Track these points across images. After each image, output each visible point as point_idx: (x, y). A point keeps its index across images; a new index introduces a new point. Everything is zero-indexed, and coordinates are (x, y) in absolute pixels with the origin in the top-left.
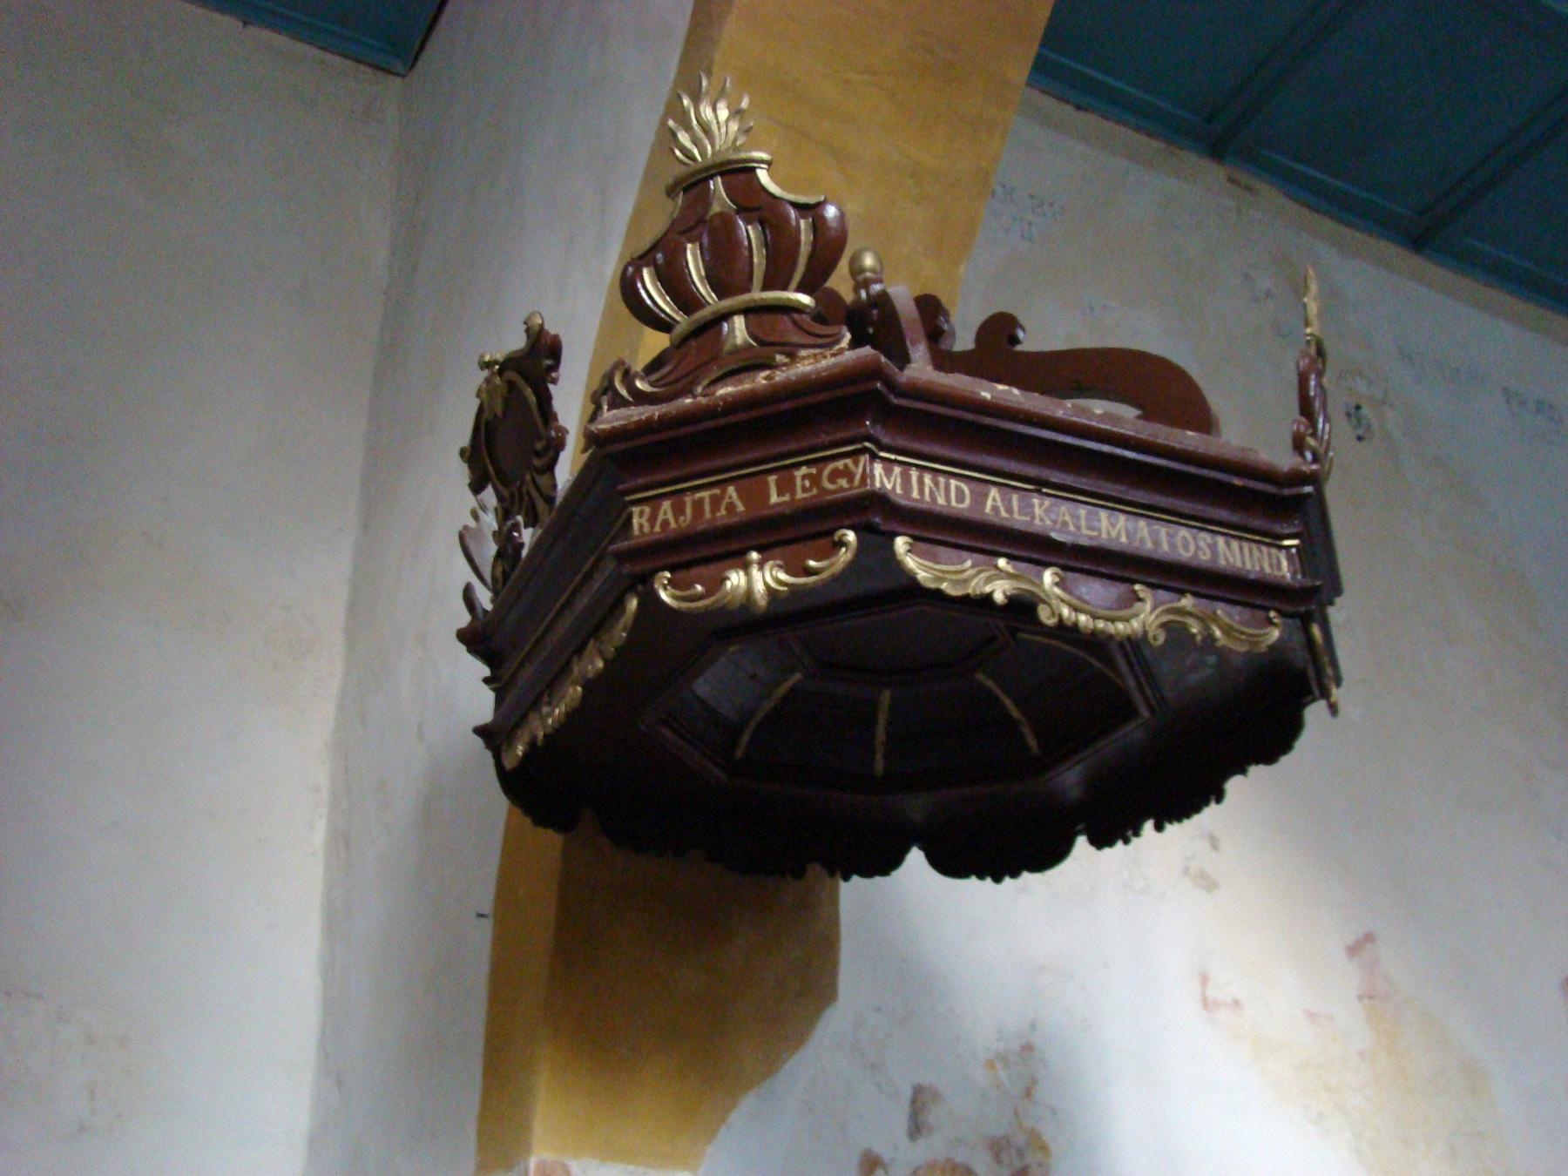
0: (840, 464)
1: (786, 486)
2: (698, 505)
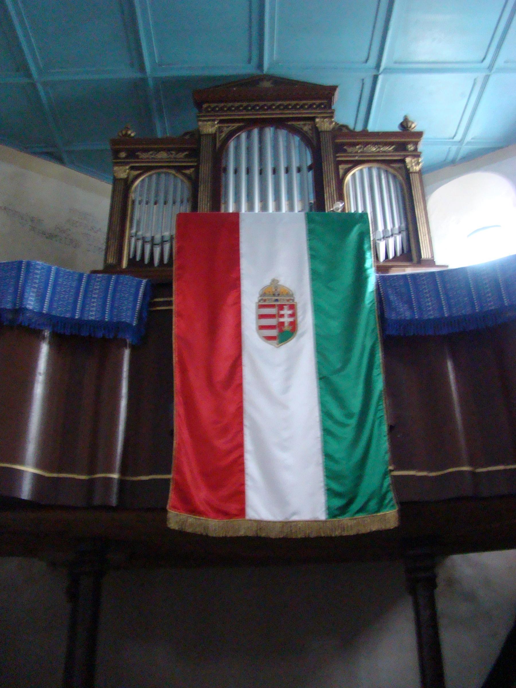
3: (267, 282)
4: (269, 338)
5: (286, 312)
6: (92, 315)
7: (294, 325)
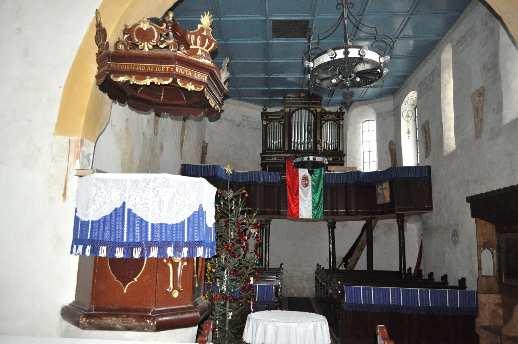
0: (204, 76)
1: (197, 75)
2: (185, 72)
3: (304, 175)
4: (303, 186)
5: (307, 181)
6: (272, 181)
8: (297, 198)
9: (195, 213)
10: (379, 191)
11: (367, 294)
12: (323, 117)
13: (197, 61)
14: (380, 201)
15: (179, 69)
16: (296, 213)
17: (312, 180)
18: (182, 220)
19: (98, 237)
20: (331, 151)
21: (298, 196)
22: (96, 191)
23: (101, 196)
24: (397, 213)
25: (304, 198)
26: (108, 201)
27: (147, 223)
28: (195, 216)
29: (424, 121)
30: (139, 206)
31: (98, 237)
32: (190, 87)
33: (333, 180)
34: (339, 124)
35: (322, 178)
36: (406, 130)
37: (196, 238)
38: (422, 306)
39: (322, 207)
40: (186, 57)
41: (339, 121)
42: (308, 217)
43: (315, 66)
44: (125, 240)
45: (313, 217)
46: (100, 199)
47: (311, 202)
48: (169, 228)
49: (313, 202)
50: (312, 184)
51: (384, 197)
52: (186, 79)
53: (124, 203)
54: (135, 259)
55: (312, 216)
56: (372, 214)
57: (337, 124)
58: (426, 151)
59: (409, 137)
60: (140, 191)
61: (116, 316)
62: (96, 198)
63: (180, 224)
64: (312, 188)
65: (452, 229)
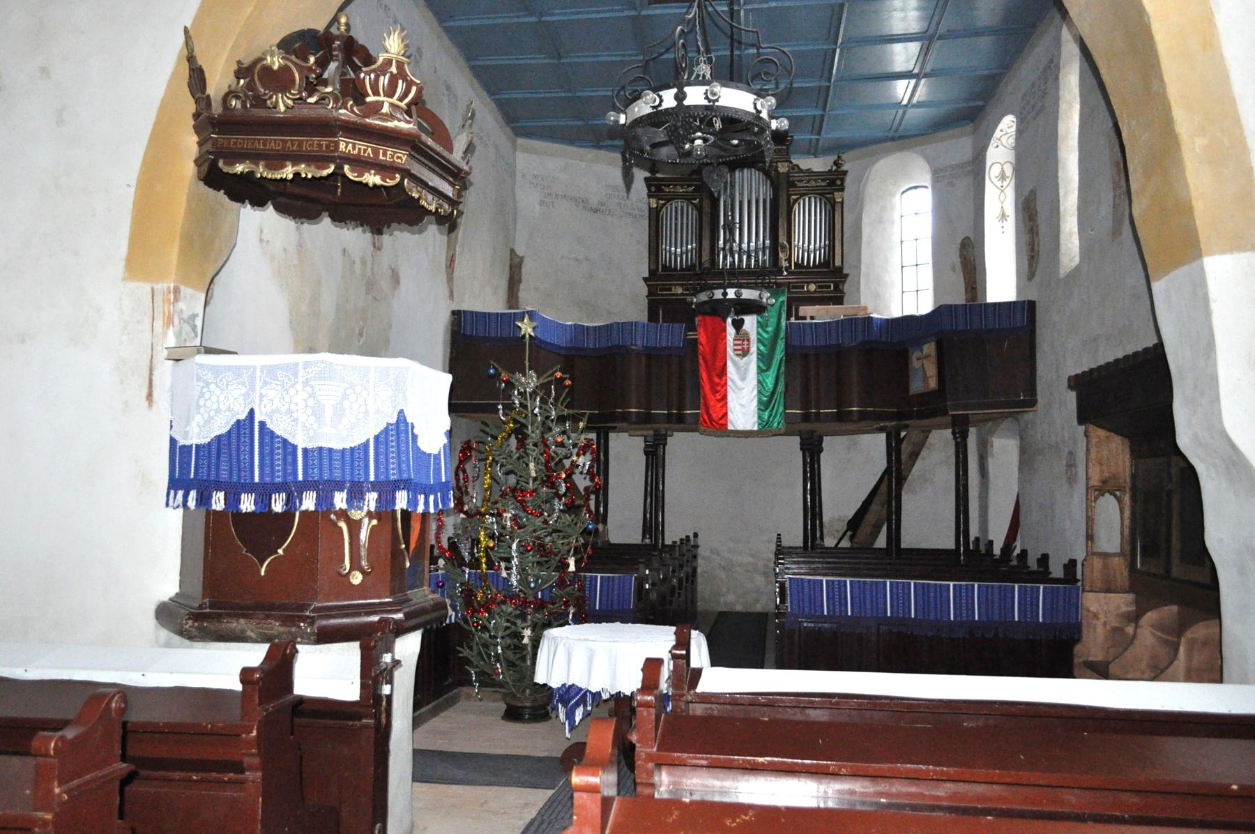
1: (385, 154)
2: (360, 149)
4: (738, 355)
5: (746, 343)
7: (748, 349)
8: (723, 382)
9: (391, 427)
10: (915, 363)
11: (901, 597)
12: (795, 186)
13: (383, 126)
14: (916, 386)
15: (346, 146)
16: (721, 419)
17: (759, 341)
18: (363, 440)
19: (208, 475)
20: (813, 268)
21: (724, 379)
22: (202, 389)
23: (210, 399)
24: (953, 416)
25: (739, 383)
26: (223, 408)
27: (295, 447)
28: (391, 433)
29: (1026, 193)
30: (278, 415)
31: (208, 475)
32: (372, 179)
33: (808, 338)
34: (832, 202)
35: (782, 334)
36: (998, 212)
37: (393, 474)
38: (958, 619)
39: (782, 403)
40: (359, 120)
41: (833, 194)
42: (749, 428)
43: (628, 122)
44: (257, 480)
45: (761, 427)
46: (209, 404)
47: (755, 392)
48: (337, 457)
49: (759, 392)
50: (758, 349)
51: (925, 378)
52: (361, 164)
53: (252, 412)
54: (277, 514)
55: (757, 424)
56: (900, 416)
57: (830, 203)
58: (1030, 266)
59: (1003, 230)
60: (280, 388)
61: (245, 616)
62: (202, 402)
63: (359, 449)
64: (758, 359)
65: (1067, 450)
